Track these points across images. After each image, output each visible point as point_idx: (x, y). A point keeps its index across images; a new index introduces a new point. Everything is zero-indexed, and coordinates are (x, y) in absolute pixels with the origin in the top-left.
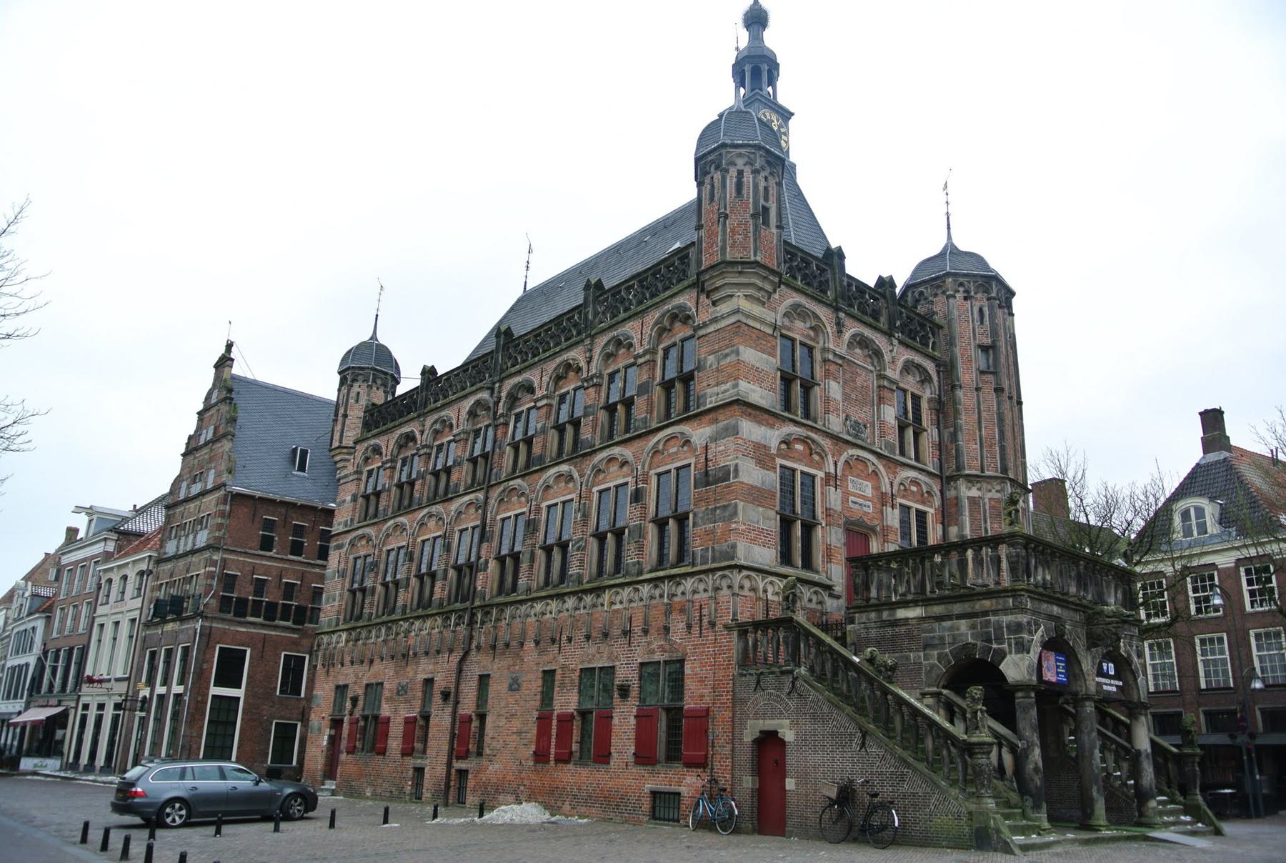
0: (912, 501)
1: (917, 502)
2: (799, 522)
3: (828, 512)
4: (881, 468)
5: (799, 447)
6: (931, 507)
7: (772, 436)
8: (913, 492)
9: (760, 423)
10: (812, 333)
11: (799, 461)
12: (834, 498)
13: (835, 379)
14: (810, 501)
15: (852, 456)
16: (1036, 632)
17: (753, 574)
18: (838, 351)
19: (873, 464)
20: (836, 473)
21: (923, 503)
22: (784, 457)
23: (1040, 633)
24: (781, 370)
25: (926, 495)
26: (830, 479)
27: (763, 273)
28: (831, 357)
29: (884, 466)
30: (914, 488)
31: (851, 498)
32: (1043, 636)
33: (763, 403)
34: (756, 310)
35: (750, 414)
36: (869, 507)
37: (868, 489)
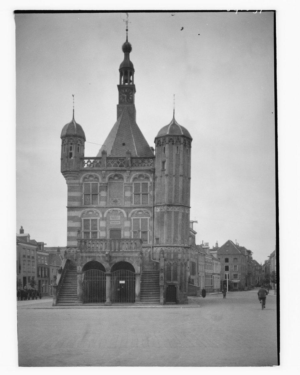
0: (139, 217)
2: (91, 233)
3: (100, 228)
4: (123, 211)
5: (91, 213)
6: (150, 216)
7: (77, 213)
8: (140, 214)
10: (96, 179)
11: (91, 216)
12: (103, 224)
13: (103, 190)
14: (95, 227)
17: (72, 248)
18: (104, 183)
19: (120, 210)
20: (103, 216)
25: (147, 214)
26: (103, 219)
27: (69, 172)
28: (102, 185)
29: (125, 210)
31: (111, 222)
34: (73, 181)
37: (119, 217)
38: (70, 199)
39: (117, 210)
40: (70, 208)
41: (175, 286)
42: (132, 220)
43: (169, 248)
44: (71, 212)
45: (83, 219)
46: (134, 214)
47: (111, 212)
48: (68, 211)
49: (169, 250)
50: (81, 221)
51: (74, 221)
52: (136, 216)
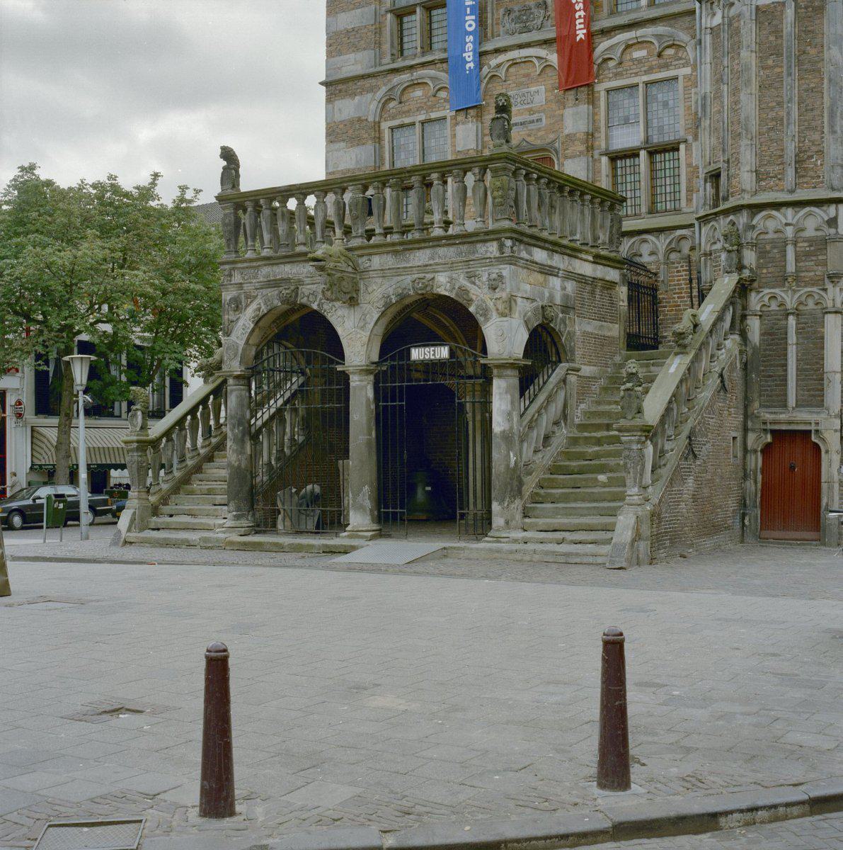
0: (636, 74)
1: (650, 70)
8: (640, 61)
9: (353, 95)
15: (499, 66)
16: (247, 306)
21: (666, 66)
22: (393, 118)
23: (254, 306)
24: (391, 11)
25: (671, 52)
30: (639, 54)
32: (259, 309)
33: (358, 70)
35: (340, 91)
36: (539, 120)
38: (337, 43)
39: (527, 61)
40: (335, 87)
41: (814, 438)
42: (603, 94)
43: (770, 217)
44: (339, 104)
45: (385, 126)
46: (611, 64)
47: (502, 73)
48: (329, 100)
49: (771, 225)
50: (379, 139)
51: (355, 141)
52: (617, 75)
